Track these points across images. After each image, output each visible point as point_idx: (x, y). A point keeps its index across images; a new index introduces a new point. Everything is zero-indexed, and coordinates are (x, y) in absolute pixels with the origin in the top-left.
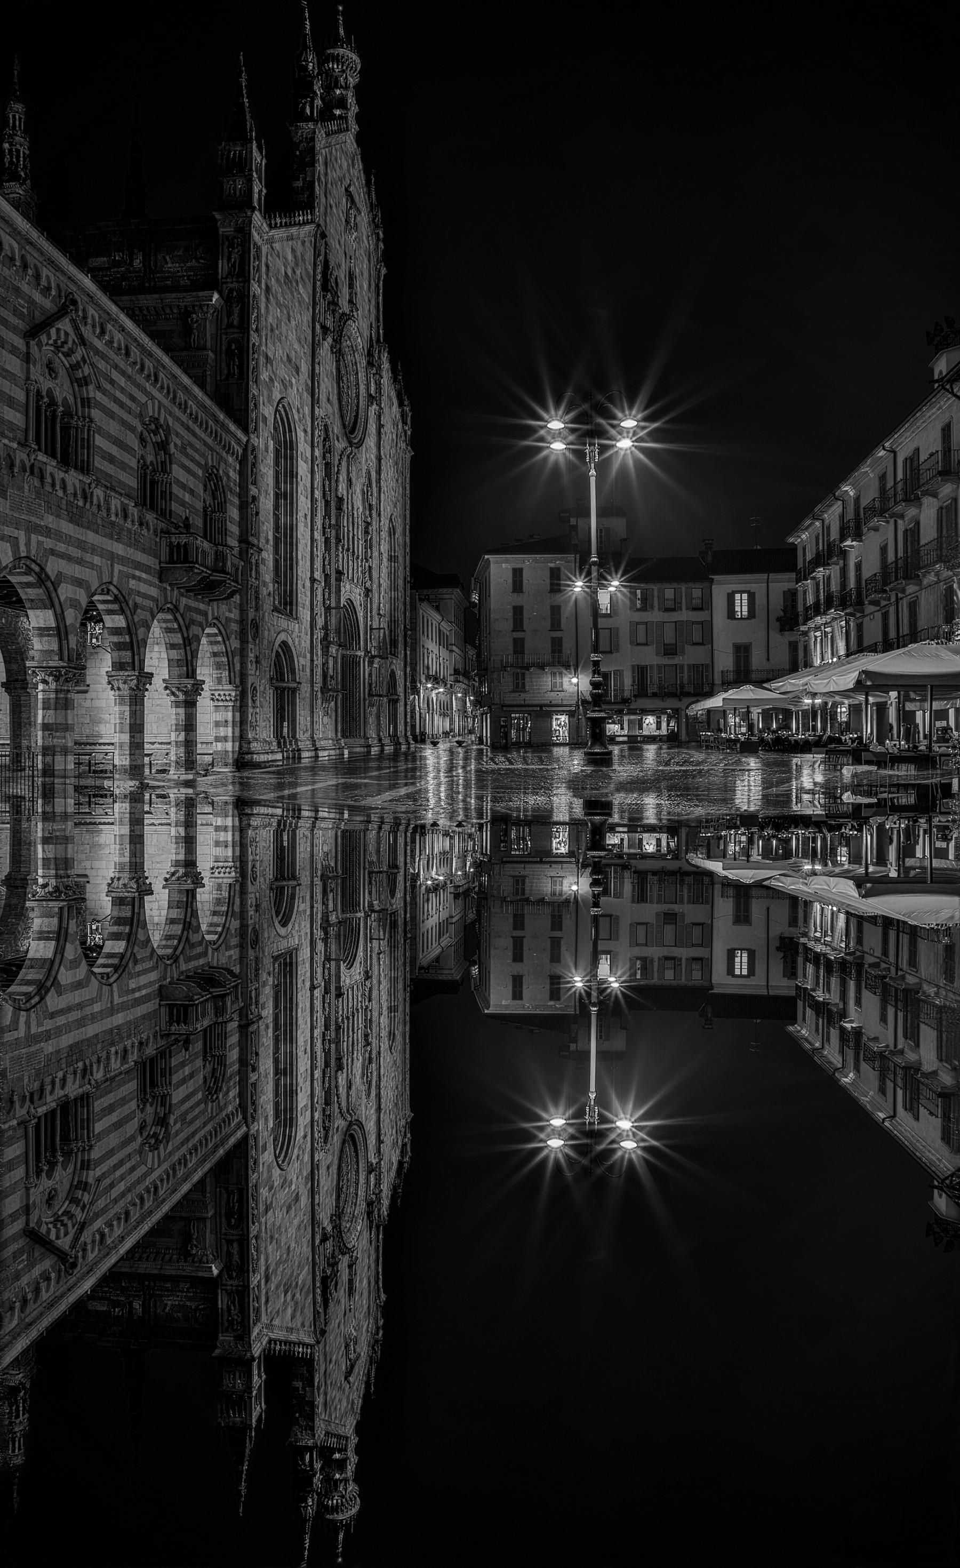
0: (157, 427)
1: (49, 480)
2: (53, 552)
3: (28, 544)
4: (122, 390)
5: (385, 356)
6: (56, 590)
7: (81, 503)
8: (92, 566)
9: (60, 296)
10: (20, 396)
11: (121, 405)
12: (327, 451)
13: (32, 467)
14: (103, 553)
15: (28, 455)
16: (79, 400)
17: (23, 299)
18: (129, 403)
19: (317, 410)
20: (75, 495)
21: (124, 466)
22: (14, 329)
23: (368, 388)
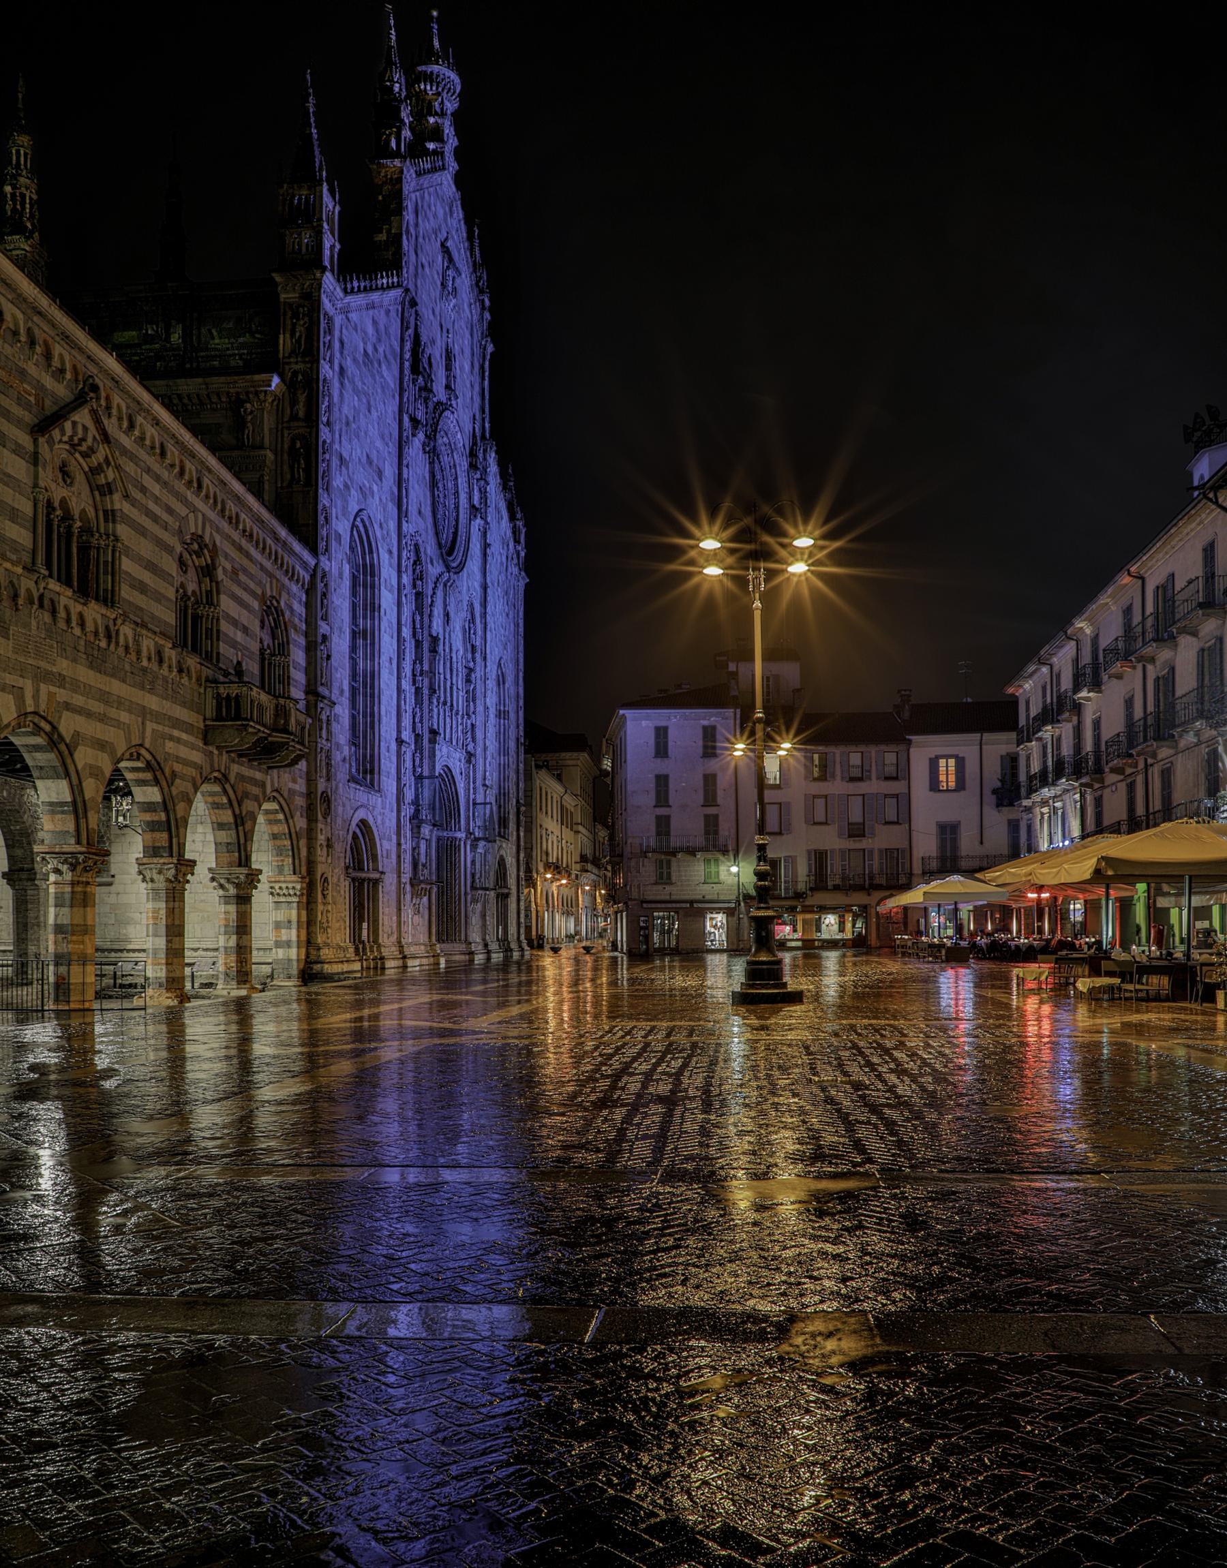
0: (200, 547)
1: (62, 614)
2: (67, 706)
3: (36, 697)
4: (157, 500)
5: (492, 458)
6: (71, 755)
7: (103, 644)
8: (118, 724)
9: (77, 380)
10: (26, 507)
11: (155, 519)
12: (418, 577)
13: (41, 597)
14: (132, 707)
15: (36, 583)
16: (101, 514)
17: (29, 383)
18: (165, 516)
19: (405, 525)
20: (96, 633)
21: (158, 597)
22: (19, 423)
23: (470, 498)
